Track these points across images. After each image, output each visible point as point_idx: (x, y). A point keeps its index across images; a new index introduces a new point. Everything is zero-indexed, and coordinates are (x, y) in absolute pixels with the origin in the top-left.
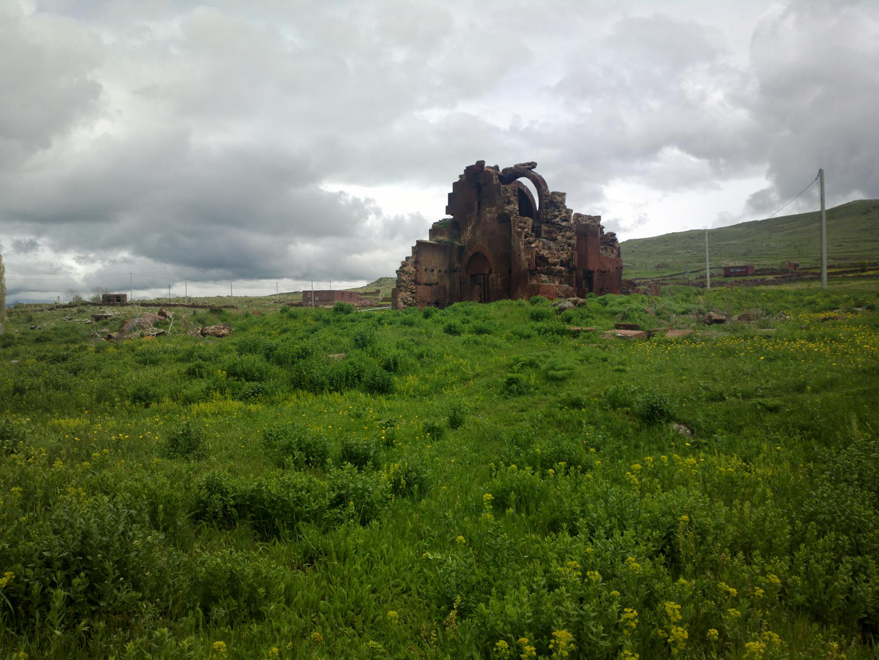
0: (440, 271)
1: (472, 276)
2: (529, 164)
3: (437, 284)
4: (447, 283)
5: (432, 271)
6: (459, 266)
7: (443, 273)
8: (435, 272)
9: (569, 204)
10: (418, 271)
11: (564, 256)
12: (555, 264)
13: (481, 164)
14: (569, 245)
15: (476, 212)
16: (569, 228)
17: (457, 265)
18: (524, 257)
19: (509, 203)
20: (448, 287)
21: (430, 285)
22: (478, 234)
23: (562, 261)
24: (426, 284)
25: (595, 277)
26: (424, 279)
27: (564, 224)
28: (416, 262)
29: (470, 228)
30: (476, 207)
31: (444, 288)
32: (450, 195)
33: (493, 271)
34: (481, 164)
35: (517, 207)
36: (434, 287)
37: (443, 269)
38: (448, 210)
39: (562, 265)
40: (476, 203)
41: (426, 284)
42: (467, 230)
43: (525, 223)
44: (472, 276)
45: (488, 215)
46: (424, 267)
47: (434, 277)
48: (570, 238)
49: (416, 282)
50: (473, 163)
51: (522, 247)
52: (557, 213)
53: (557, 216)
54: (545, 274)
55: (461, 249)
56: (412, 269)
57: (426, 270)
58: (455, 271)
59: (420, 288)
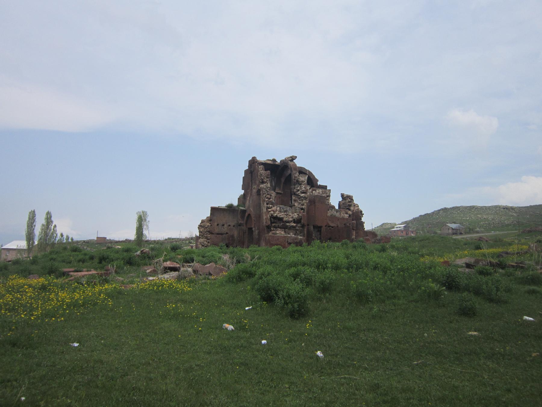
2: (291, 157)
3: (227, 233)
4: (236, 233)
5: (223, 225)
6: (242, 222)
7: (232, 227)
8: (225, 226)
10: (211, 225)
11: (296, 216)
12: (288, 222)
14: (302, 209)
16: (305, 198)
18: (265, 217)
19: (263, 182)
21: (222, 234)
23: (294, 220)
24: (218, 234)
25: (323, 229)
26: (217, 231)
27: (302, 195)
28: (210, 220)
31: (233, 236)
32: (243, 178)
35: (269, 185)
37: (232, 224)
39: (294, 223)
41: (218, 234)
43: (271, 196)
46: (216, 224)
47: (225, 229)
48: (303, 205)
49: (211, 233)
52: (299, 188)
53: (298, 190)
54: (281, 228)
55: (244, 212)
56: (208, 224)
57: (218, 225)
58: (240, 225)
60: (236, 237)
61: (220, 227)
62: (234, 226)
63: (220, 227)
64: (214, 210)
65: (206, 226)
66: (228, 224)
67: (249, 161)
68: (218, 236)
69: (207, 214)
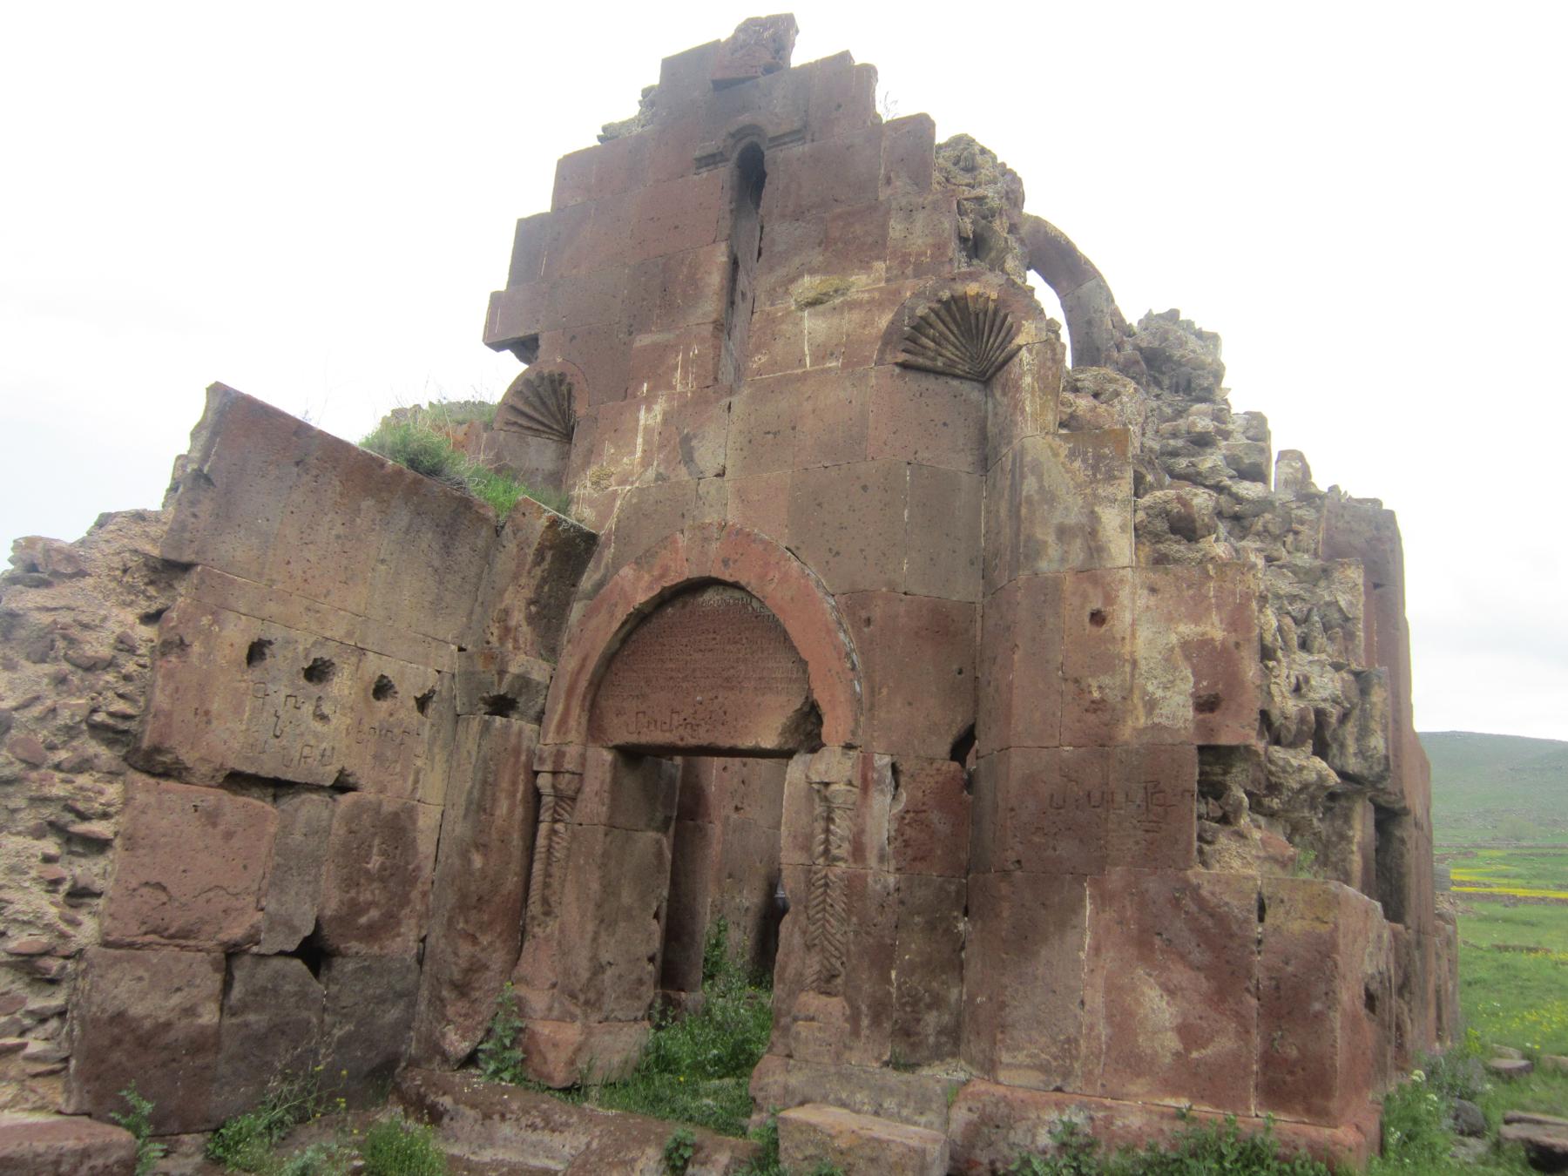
0: (382, 689)
1: (631, 756)
3: (342, 786)
5: (317, 672)
6: (540, 673)
7: (402, 708)
8: (342, 685)
9: (1242, 392)
10: (174, 646)
13: (770, 37)
15: (710, 306)
17: (524, 662)
20: (427, 820)
21: (279, 787)
22: (713, 451)
24: (237, 781)
26: (231, 737)
29: (649, 418)
30: (715, 279)
31: (397, 829)
33: (834, 728)
34: (770, 37)
36: (310, 807)
38: (510, 330)
40: (721, 256)
41: (237, 781)
42: (622, 433)
44: (631, 756)
45: (813, 326)
50: (721, 28)
51: (1121, 549)
52: (1204, 424)
56: (124, 619)
57: (256, 652)
59: (168, 808)
60: (425, 846)
61: (280, 691)
62: (422, 703)
63: (280, 691)
64: (244, 438)
65: (98, 646)
66: (374, 666)
67: (671, 67)
68: (235, 806)
69: (133, 465)
